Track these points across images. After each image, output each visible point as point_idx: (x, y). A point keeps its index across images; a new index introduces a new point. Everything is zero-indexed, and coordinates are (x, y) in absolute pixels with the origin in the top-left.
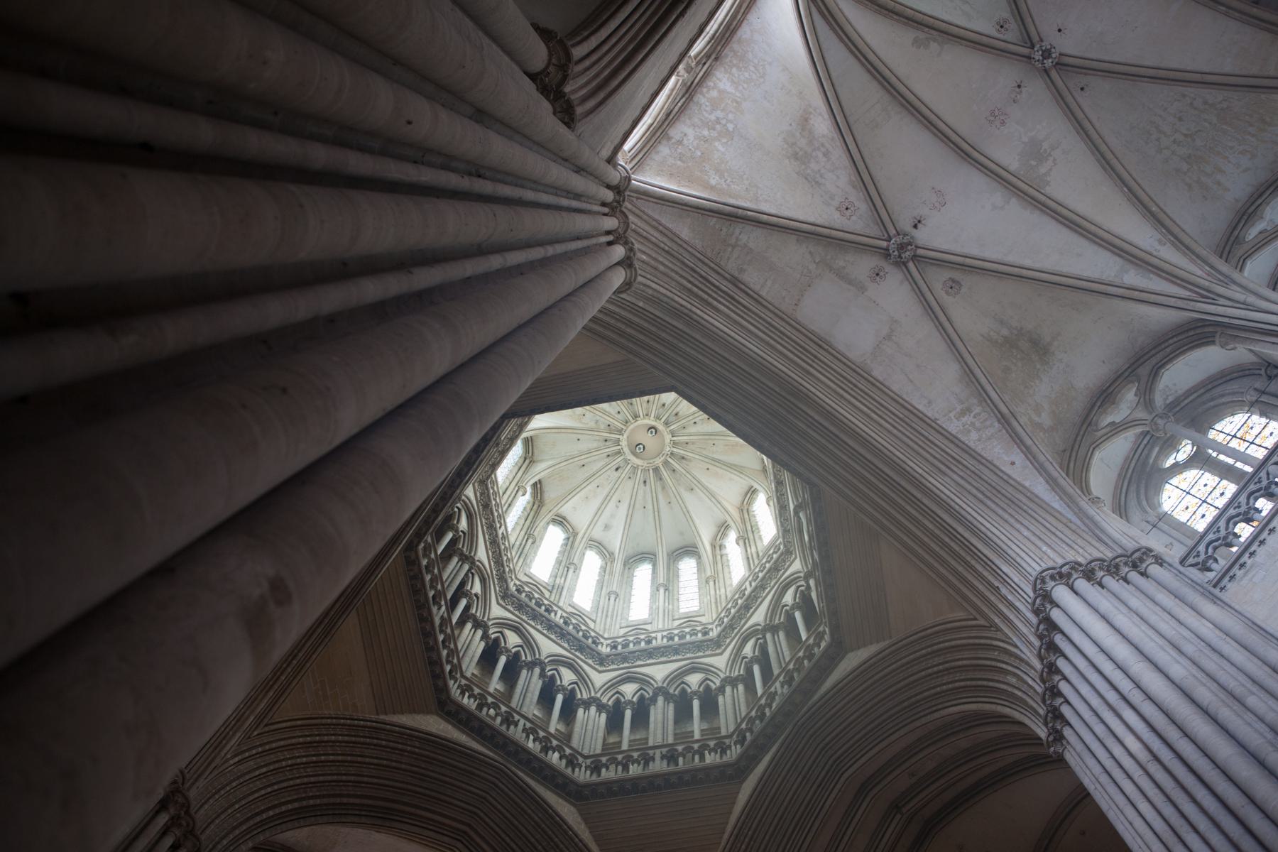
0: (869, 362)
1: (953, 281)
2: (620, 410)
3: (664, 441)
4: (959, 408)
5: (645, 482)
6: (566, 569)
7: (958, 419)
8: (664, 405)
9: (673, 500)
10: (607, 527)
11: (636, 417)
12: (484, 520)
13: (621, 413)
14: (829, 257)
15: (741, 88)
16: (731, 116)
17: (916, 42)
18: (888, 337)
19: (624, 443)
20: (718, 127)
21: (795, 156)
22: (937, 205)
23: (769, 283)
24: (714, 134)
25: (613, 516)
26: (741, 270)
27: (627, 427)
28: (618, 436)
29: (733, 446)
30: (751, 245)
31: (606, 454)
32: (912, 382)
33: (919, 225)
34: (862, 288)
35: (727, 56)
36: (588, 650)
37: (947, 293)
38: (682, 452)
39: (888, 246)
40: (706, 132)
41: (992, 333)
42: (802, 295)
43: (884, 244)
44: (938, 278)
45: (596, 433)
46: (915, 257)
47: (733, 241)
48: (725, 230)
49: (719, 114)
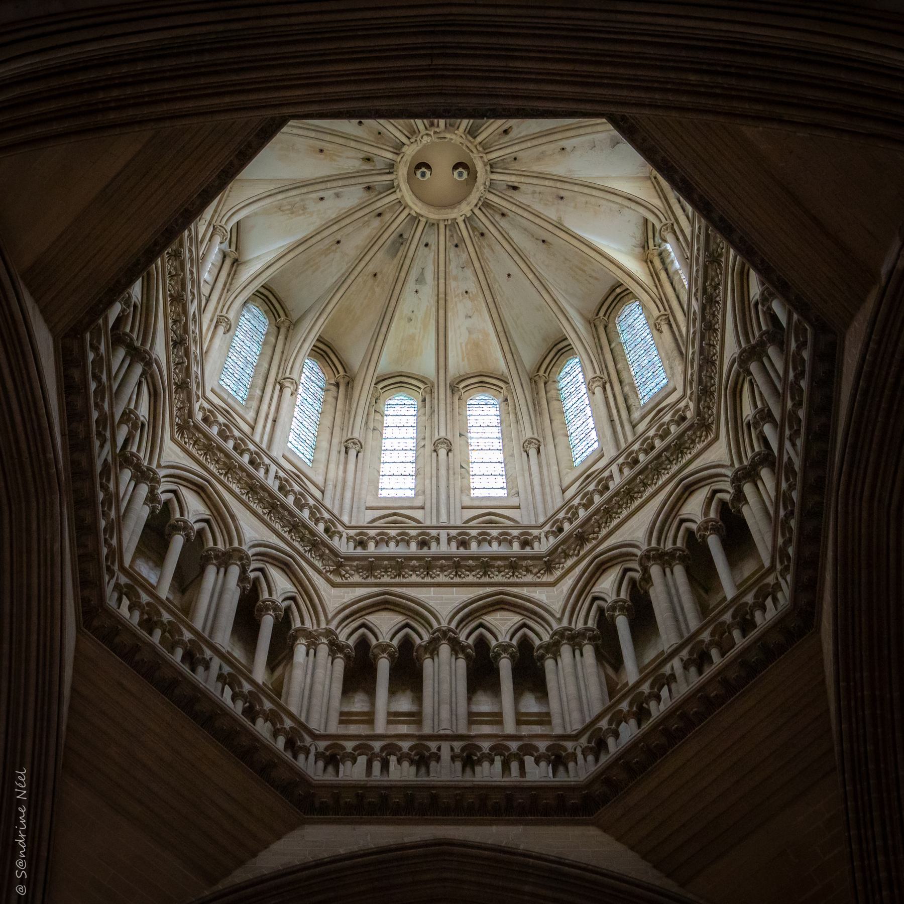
2: (422, 246)
3: (419, 151)
8: (369, 188)
11: (415, 219)
12: (604, 532)
13: (424, 240)
19: (465, 209)
27: (439, 220)
28: (462, 226)
31: (503, 223)
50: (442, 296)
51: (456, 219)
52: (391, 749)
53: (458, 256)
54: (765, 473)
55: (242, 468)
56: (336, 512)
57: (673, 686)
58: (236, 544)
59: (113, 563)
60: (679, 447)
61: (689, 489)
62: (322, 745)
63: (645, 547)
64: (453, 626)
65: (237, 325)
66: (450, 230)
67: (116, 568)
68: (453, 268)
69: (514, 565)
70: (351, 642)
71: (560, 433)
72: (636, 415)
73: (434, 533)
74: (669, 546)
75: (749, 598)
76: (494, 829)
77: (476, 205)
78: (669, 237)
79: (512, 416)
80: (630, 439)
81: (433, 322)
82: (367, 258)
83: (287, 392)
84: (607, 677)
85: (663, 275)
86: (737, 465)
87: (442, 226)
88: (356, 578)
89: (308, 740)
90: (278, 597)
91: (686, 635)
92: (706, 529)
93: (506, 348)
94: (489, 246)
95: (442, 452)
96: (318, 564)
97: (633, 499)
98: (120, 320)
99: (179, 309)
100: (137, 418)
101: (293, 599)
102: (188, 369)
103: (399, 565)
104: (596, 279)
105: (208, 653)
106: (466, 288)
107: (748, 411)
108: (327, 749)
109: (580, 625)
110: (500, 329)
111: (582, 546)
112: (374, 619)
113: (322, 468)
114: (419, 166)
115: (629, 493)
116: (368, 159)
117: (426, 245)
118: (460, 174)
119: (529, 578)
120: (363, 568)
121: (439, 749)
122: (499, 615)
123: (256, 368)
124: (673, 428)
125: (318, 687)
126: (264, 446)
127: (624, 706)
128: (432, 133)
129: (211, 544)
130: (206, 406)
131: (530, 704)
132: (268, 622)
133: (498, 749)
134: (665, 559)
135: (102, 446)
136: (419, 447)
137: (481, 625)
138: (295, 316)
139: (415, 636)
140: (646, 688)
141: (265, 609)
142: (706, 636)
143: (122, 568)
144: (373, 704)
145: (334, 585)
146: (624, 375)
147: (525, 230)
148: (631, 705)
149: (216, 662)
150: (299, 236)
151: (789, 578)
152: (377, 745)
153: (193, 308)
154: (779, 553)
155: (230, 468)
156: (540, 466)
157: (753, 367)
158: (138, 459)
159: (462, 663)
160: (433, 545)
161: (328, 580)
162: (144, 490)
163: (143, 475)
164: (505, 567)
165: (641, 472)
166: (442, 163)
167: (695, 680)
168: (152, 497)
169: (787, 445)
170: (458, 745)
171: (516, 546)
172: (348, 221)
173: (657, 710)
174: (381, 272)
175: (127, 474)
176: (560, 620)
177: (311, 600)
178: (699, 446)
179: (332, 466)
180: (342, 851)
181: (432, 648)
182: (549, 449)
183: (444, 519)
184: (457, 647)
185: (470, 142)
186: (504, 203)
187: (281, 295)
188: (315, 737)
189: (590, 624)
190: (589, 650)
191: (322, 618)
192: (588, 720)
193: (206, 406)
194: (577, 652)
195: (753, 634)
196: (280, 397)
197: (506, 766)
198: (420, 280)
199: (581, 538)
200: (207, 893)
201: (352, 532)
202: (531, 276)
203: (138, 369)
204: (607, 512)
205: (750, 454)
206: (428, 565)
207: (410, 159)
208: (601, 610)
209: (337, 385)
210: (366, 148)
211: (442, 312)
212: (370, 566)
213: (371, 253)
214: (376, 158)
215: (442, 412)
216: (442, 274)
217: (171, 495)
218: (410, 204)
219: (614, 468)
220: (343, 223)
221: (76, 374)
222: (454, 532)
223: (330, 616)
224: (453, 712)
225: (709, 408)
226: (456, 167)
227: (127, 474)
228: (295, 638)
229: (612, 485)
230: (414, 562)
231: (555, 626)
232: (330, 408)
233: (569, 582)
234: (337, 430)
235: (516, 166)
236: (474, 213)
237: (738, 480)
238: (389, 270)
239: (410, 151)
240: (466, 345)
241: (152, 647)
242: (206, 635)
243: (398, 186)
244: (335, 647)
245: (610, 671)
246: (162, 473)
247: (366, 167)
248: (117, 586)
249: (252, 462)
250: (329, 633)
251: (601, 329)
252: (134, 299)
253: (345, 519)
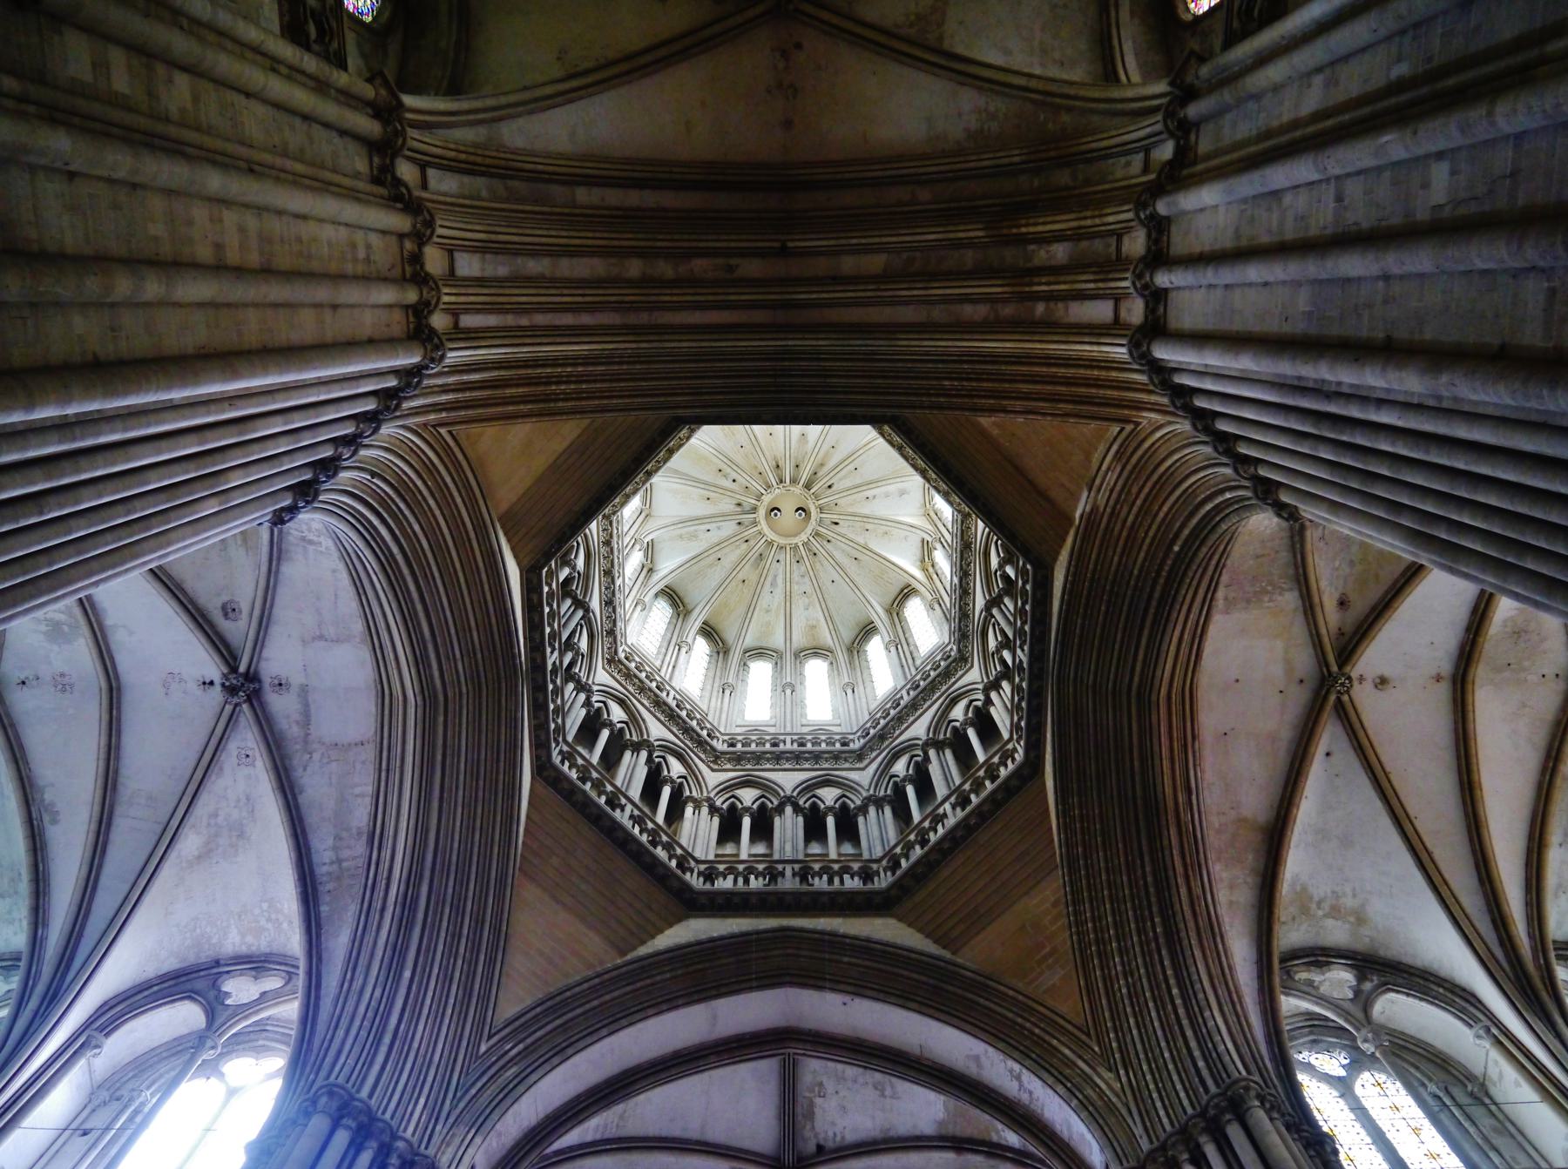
0: (358, 640)
1: (226, 615)
4: (311, 548)
5: (830, 487)
7: (320, 543)
8: (739, 523)
9: (826, 447)
10: (902, 493)
11: (770, 543)
12: (897, 732)
14: (298, 747)
15: (225, 924)
16: (257, 911)
17: (54, 822)
18: (321, 637)
19: (804, 537)
20: (273, 916)
21: (241, 835)
22: (177, 679)
23: (357, 790)
24: (281, 918)
25: (887, 495)
26: (359, 834)
28: (801, 548)
30: (330, 842)
31: (828, 546)
32: (336, 595)
33: (208, 681)
34: (304, 690)
35: (207, 957)
36: (966, 538)
37: (241, 612)
38: (771, 476)
39: (245, 702)
40: (285, 925)
41: (239, 542)
42: (350, 745)
43: (245, 707)
44: (237, 630)
45: (811, 573)
46: (234, 669)
47: (335, 867)
48: (329, 886)
49: (263, 922)
50: (788, 593)
52: (750, 870)
53: (799, 569)
54: (1005, 684)
55: (650, 690)
56: (715, 724)
57: (945, 821)
58: (645, 737)
59: (559, 736)
60: (947, 674)
61: (954, 702)
62: (702, 867)
63: (924, 738)
64: (795, 794)
65: (651, 608)
67: (561, 739)
68: (796, 577)
69: (836, 757)
70: (725, 806)
71: (867, 680)
72: (918, 662)
73: (782, 737)
74: (942, 737)
75: (996, 760)
76: (822, 920)
78: (938, 546)
79: (836, 672)
80: (914, 673)
81: (782, 611)
82: (738, 569)
83: (684, 650)
84: (900, 826)
85: (935, 576)
86: (985, 681)
87: (788, 548)
88: (729, 766)
89: (693, 864)
90: (674, 775)
91: (953, 788)
92: (966, 724)
93: (831, 627)
95: (788, 692)
96: (703, 756)
97: (916, 710)
98: (568, 581)
99: (610, 580)
100: (579, 648)
101: (685, 777)
102: (615, 621)
103: (758, 758)
105: (623, 801)
107: (992, 644)
108: (706, 869)
109: (882, 793)
110: (827, 614)
111: (882, 743)
112: (740, 793)
113: (706, 701)
114: (772, 510)
115: (914, 706)
116: (739, 505)
118: (800, 515)
119: (847, 765)
120: (733, 759)
121: (784, 869)
122: (826, 789)
123: (663, 637)
124: (942, 663)
125: (701, 833)
126: (667, 679)
127: (912, 837)
129: (628, 737)
130: (627, 650)
131: (848, 849)
132: (666, 792)
133: (826, 870)
134: (939, 746)
135: (552, 653)
136: (774, 690)
137: (814, 796)
138: (690, 607)
139: (768, 803)
140: (926, 824)
141: (665, 782)
142: (967, 787)
143: (565, 741)
144: (739, 849)
145: (713, 770)
146: (910, 640)
148: (916, 836)
149: (629, 808)
150: (693, 554)
151: (1022, 743)
152: (741, 867)
153: (618, 582)
154: (1015, 727)
155: (642, 689)
156: (854, 700)
157: (995, 611)
158: (579, 676)
159: (801, 819)
160: (782, 745)
161: (709, 767)
162: (582, 697)
163: (581, 687)
164: (831, 758)
165: (921, 692)
166: (788, 508)
167: (960, 814)
168: (587, 703)
169: (1019, 651)
170: (797, 867)
171: (838, 745)
172: (726, 544)
173: (933, 837)
175: (571, 686)
176: (868, 790)
177: (697, 779)
178: (960, 673)
179: (714, 700)
180: (715, 935)
181: (780, 810)
182: (860, 689)
183: (788, 730)
184: (797, 809)
186: (829, 533)
187: (681, 595)
188: (698, 862)
189: (889, 792)
190: (888, 810)
191: (704, 790)
192: (887, 849)
193: (627, 650)
194: (880, 811)
195: (999, 781)
196: (678, 654)
197: (831, 881)
198: (774, 584)
199: (882, 737)
200: (619, 961)
201: (726, 738)
202: (848, 580)
203: (580, 613)
204: (900, 719)
205: (994, 673)
206: (778, 757)
208: (895, 783)
209: (718, 653)
210: (738, 496)
211: (788, 604)
212: (738, 759)
213: (741, 566)
214: (745, 504)
215: (788, 667)
216: (788, 580)
217: (601, 705)
218: (767, 533)
219: (904, 692)
220: (722, 545)
221: (535, 597)
222: (795, 737)
223: (710, 789)
224: (795, 848)
225: (966, 647)
226: (797, 511)
227: (571, 686)
228: (684, 804)
229: (902, 702)
230: (768, 755)
231: (865, 794)
232: (713, 666)
233: (874, 766)
234: (717, 679)
235: (837, 508)
237: (986, 691)
238: (753, 577)
239: (767, 499)
241: (584, 792)
242: (624, 790)
244: (713, 810)
245: (903, 826)
246: (595, 688)
247: (739, 509)
248: (561, 752)
249: (658, 687)
250: (709, 799)
251: (895, 615)
252: (578, 568)
253: (722, 730)
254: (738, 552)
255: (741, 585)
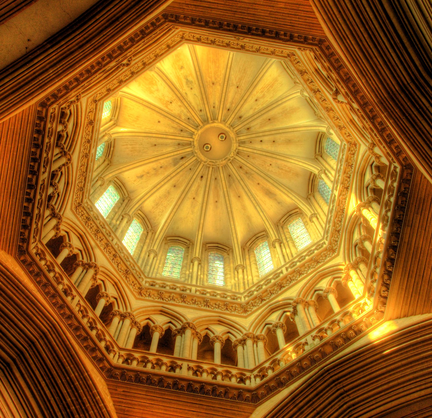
2: (202, 109)
5: (202, 177)
6: (121, 217)
9: (222, 200)
11: (214, 119)
19: (196, 137)
27: (204, 125)
28: (193, 130)
29: (286, 171)
45: (177, 121)
51: (198, 131)
66: (196, 123)
77: (193, 142)
87: (201, 124)
94: (176, 128)
104: (124, 145)
106: (173, 104)
117: (201, 110)
128: (231, 159)
147: (166, 145)
174: (212, 87)
185: (213, 165)
207: (233, 142)
236: (191, 138)
240: (156, 82)
243: (230, 128)
254: (230, 100)
255: (213, 79)
